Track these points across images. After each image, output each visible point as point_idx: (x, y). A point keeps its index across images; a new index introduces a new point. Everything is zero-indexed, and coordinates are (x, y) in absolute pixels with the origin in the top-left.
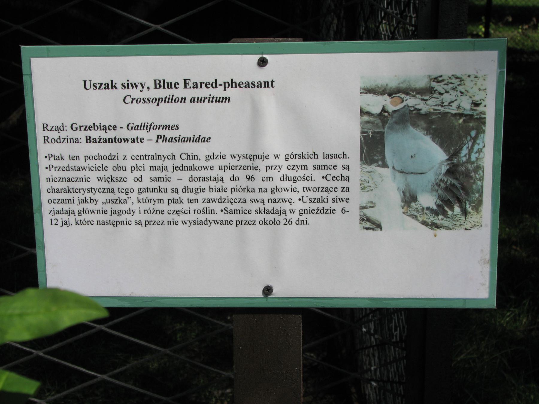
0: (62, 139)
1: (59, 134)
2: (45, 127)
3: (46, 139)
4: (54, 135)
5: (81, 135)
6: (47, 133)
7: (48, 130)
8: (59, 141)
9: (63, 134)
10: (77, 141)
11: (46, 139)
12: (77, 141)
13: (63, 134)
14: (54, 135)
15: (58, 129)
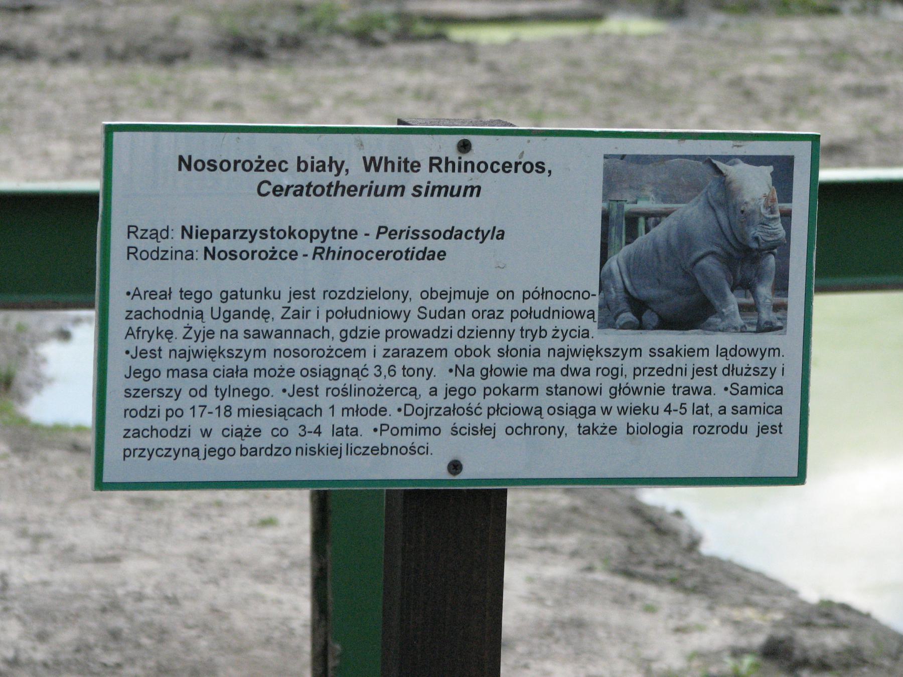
0: (162, 251)
1: (159, 244)
2: (131, 231)
3: (131, 252)
4: (149, 245)
5: (197, 245)
6: (133, 241)
7: (137, 237)
8: (160, 255)
9: (164, 245)
10: (190, 256)
11: (131, 252)
12: (190, 256)
13: (164, 245)
14: (149, 245)
15: (155, 235)
